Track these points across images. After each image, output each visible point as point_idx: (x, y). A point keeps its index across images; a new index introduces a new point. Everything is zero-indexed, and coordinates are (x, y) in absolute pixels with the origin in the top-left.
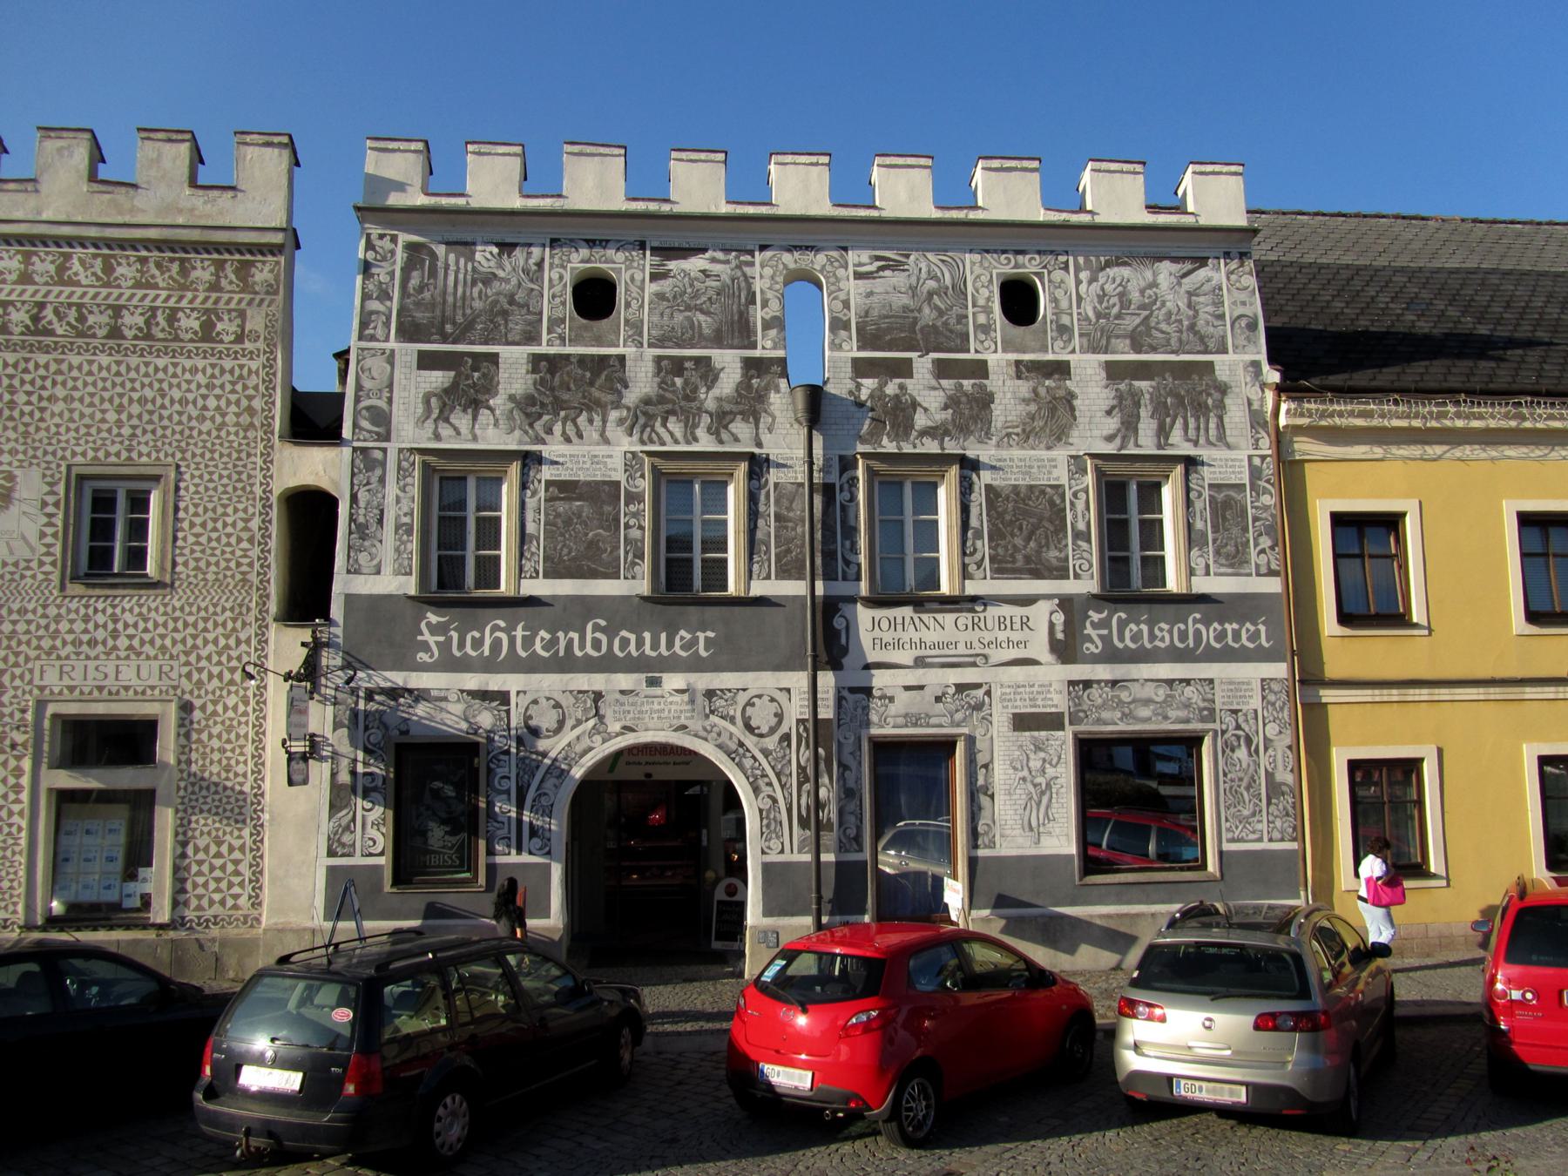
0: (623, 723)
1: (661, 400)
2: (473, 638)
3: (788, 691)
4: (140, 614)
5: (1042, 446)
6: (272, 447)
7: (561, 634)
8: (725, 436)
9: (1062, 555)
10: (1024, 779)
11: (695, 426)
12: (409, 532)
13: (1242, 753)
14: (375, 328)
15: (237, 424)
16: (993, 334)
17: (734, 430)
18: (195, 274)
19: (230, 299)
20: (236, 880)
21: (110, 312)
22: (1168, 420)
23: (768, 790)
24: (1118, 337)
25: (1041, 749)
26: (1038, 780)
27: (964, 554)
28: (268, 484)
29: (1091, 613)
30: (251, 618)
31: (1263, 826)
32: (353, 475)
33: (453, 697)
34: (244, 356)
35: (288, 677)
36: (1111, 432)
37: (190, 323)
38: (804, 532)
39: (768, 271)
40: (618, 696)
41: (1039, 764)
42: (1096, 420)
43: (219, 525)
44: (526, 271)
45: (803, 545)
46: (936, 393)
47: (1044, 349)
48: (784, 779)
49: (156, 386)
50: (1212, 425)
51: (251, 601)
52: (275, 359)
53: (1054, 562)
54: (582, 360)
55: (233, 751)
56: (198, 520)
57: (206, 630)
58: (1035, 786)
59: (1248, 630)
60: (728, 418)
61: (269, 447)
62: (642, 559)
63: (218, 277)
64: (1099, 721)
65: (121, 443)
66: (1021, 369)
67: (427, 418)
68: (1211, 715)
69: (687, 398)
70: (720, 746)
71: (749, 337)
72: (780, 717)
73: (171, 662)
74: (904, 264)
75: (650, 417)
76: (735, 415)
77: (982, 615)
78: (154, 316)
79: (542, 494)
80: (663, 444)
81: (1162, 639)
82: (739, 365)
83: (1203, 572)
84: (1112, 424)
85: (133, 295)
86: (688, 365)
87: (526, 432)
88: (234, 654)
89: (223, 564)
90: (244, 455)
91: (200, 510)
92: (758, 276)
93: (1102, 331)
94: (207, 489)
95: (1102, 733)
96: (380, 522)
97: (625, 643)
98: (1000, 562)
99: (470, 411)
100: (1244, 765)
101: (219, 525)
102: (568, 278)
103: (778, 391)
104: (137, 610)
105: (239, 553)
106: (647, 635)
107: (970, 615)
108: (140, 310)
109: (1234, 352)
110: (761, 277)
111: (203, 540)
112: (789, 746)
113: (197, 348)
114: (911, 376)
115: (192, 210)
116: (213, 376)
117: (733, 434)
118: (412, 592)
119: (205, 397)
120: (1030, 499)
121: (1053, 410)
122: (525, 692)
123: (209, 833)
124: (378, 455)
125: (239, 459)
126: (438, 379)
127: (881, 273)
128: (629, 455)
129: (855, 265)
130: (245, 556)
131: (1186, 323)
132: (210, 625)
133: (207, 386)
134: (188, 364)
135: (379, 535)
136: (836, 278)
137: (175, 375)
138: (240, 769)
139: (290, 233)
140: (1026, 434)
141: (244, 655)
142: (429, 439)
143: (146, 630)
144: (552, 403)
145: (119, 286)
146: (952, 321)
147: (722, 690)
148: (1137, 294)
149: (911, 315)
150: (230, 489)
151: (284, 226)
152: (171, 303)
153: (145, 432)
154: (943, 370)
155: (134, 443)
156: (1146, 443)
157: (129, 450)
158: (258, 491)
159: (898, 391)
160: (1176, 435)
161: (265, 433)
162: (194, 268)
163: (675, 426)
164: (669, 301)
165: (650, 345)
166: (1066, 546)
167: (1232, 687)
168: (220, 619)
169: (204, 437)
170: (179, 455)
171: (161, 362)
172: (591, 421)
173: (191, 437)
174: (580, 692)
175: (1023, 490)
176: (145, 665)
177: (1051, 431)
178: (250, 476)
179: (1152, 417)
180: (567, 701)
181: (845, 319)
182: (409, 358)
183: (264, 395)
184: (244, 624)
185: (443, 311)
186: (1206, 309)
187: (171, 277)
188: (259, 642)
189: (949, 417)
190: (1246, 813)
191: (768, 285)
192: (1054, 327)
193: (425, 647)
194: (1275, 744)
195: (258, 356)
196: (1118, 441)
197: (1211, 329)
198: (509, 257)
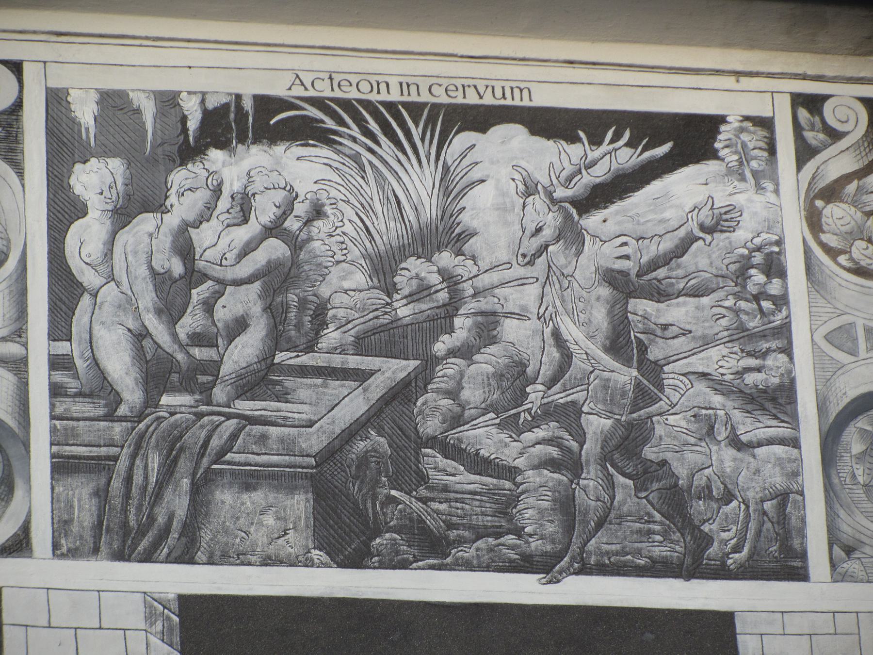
109: (838, 575)
148: (359, 279)
186: (697, 363)
197: (727, 457)
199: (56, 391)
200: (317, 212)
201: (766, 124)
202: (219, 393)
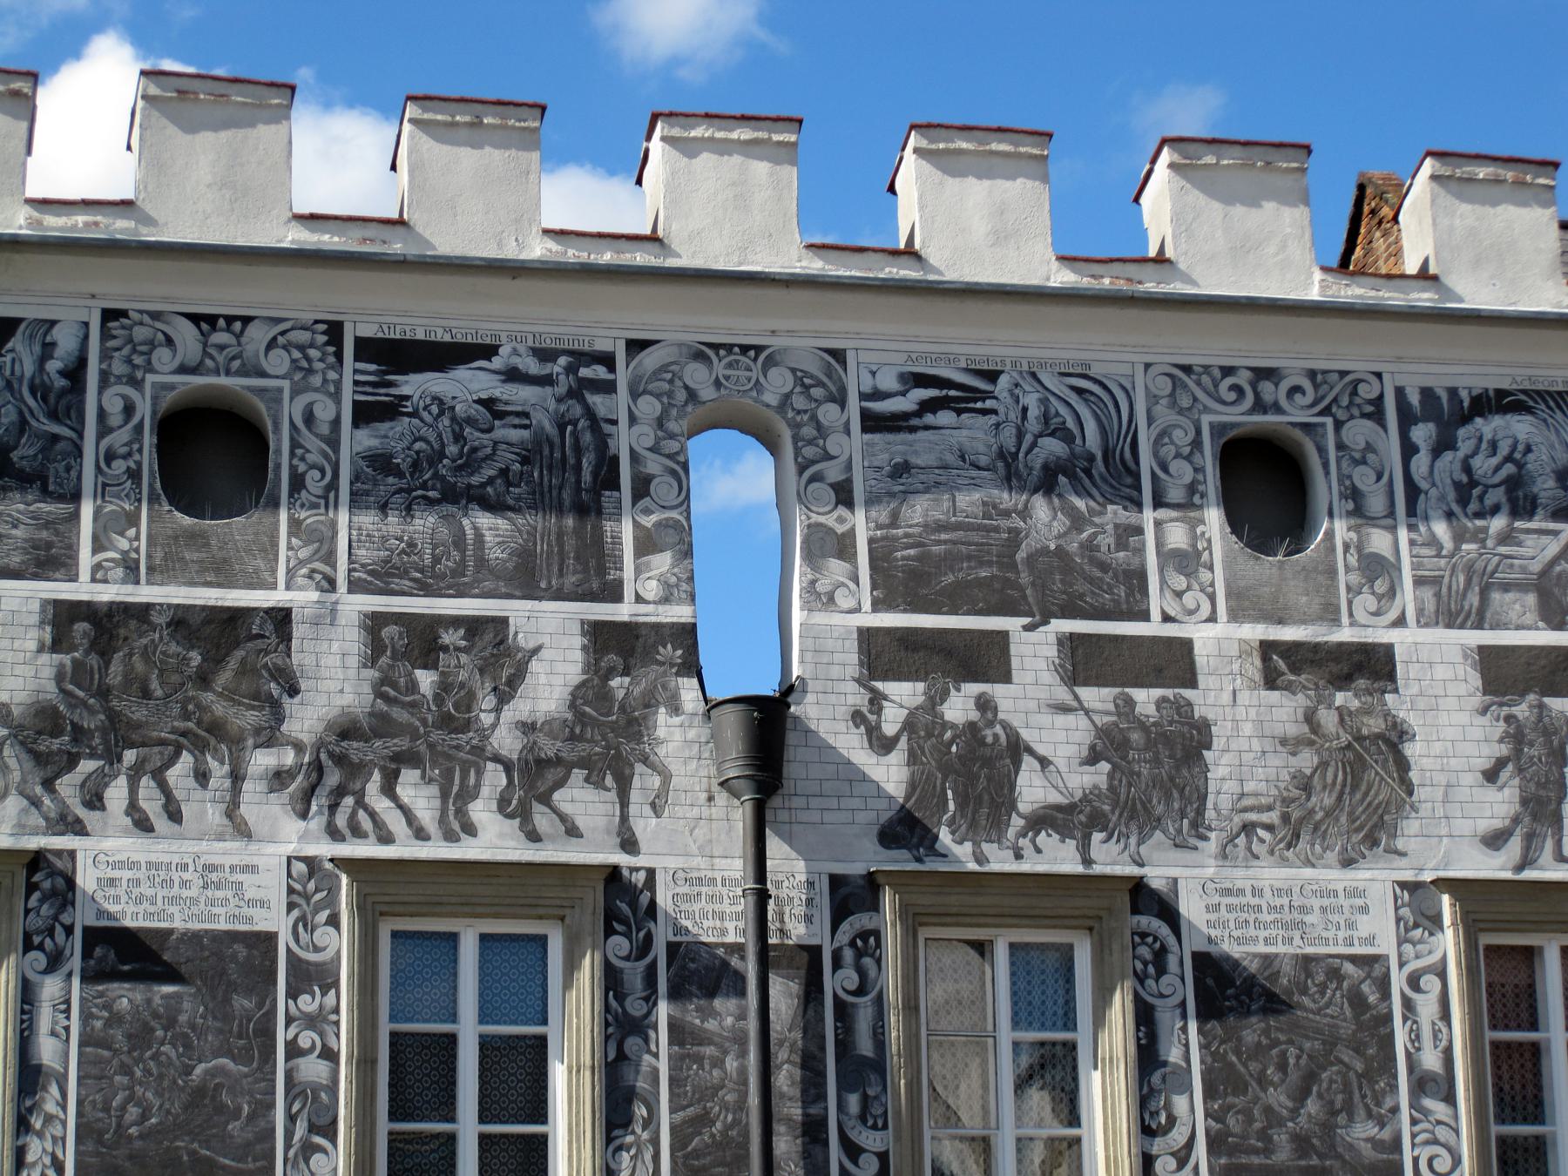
1: (381, 726)
8: (542, 819)
9: (1386, 1134)
11: (469, 794)
16: (1205, 575)
17: (566, 808)
24: (1506, 587)
27: (1147, 1131)
36: (1498, 824)
38: (743, 1071)
39: (649, 407)
42: (1462, 794)
44: (40, 389)
45: (741, 1105)
46: (1070, 720)
47: (1330, 615)
53: (1367, 1151)
54: (183, 621)
60: (551, 775)
62: (330, 1132)
69: (447, 722)
71: (602, 571)
74: (986, 395)
75: (354, 771)
76: (572, 765)
79: (76, 962)
80: (386, 838)
82: (578, 641)
84: (1500, 804)
86: (449, 637)
87: (35, 803)
93: (1470, 570)
98: (1233, 1151)
102: (144, 409)
103: (676, 709)
110: (633, 420)
114: (1006, 678)
117: (563, 818)
120: (1304, 991)
121: (1355, 769)
127: (929, 419)
128: (300, 868)
129: (863, 397)
136: (819, 426)
144: (104, 733)
146: (1106, 540)
148: (1551, 483)
149: (1004, 523)
159: (974, 715)
163: (417, 793)
164: (400, 475)
165: (355, 587)
166: (1395, 1110)
172: (202, 777)
175: (1287, 968)
177: (1352, 819)
181: (840, 529)
191: (650, 443)
192: (1353, 560)
196: (1515, 846)
199: (1412, 543)
200: (1528, 449)
202: (1490, 543)
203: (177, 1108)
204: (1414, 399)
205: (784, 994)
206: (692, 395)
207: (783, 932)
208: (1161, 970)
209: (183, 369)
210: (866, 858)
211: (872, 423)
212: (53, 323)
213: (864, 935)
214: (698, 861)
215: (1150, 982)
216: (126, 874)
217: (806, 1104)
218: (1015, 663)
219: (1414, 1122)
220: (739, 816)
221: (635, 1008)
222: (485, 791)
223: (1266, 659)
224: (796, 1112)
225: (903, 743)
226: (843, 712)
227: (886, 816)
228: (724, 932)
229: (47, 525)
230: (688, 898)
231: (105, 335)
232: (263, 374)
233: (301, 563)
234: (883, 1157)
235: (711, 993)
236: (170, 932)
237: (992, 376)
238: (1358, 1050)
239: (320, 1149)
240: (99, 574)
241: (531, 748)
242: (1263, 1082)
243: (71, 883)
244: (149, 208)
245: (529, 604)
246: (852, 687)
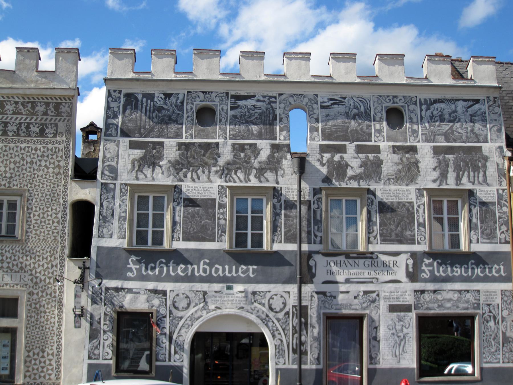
0: (216, 305)
1: (234, 163)
2: (151, 266)
3: (289, 292)
4: (12, 253)
5: (404, 184)
6: (68, 182)
7: (189, 266)
8: (262, 179)
9: (412, 234)
10: (393, 334)
11: (249, 174)
12: (125, 220)
13: (492, 324)
14: (111, 131)
15: (53, 172)
16: (383, 134)
17: (267, 177)
18: (37, 108)
19: (52, 119)
20: (50, 368)
21: (3, 125)
22: (461, 173)
23: (278, 336)
24: (439, 135)
25: (401, 321)
26: (400, 334)
27: (369, 233)
28: (66, 198)
29: (425, 260)
30: (58, 256)
31: (500, 356)
32: (101, 195)
33: (142, 292)
34: (56, 143)
35: (75, 282)
36: (435, 178)
37: (35, 129)
38: (296, 222)
39: (282, 105)
40: (214, 293)
41: (400, 327)
42: (429, 173)
43: (45, 216)
44: (176, 106)
45: (296, 228)
46: (357, 160)
48: (286, 332)
49: (21, 156)
50: (481, 175)
51: (58, 248)
52: (69, 145)
53: (409, 237)
54: (200, 145)
55: (49, 312)
56: (37, 214)
57: (39, 260)
58: (398, 337)
59: (495, 268)
60: (264, 171)
61: (66, 182)
62: (225, 232)
63: (47, 110)
64: (428, 308)
65: (6, 180)
66: (396, 150)
67: (133, 170)
68: (478, 306)
69: (246, 162)
70: (258, 317)
71: (273, 135)
72: (285, 304)
73: (25, 274)
74: (343, 102)
75: (230, 171)
76: (267, 169)
77: (376, 260)
78: (20, 126)
79: (182, 204)
80: (235, 182)
81: (457, 272)
82: (269, 147)
83: (476, 241)
84: (436, 174)
85: (12, 118)
86: (246, 147)
87: (175, 177)
88: (51, 271)
89: (47, 232)
90: (56, 186)
91: (38, 209)
92: (278, 108)
93: (432, 132)
94: (40, 200)
95: (429, 314)
96: (112, 215)
97: (217, 270)
98: (384, 236)
99: (151, 167)
100: (493, 329)
101: (45, 216)
102: (194, 109)
103: (286, 159)
104: (11, 251)
105: (53, 228)
106: (227, 267)
107: (370, 260)
108: (15, 124)
109: (491, 142)
110: (279, 108)
111: (39, 222)
112: (289, 317)
113: (38, 140)
114: (346, 153)
115: (37, 81)
116: (44, 152)
117: (266, 178)
118: (126, 246)
119: (40, 161)
120: (398, 208)
121: (409, 168)
122: (173, 291)
123: (39, 347)
124: (112, 186)
125: (54, 187)
126: (138, 153)
127: (333, 106)
129: (321, 103)
130: (56, 229)
131: (469, 129)
132: (41, 258)
133: (41, 156)
134: (34, 146)
135: (112, 221)
136: (313, 108)
137: (28, 151)
138: (52, 320)
139: (76, 90)
140: (398, 178)
141: (55, 272)
142: (134, 180)
143: (15, 260)
145: (7, 114)
146: (365, 128)
147: (259, 292)
150: (50, 200)
151: (74, 88)
152: (28, 121)
153: (16, 175)
154: (360, 150)
155: (11, 180)
156: (451, 183)
157: (9, 183)
158: (61, 201)
159: (340, 159)
160: (465, 180)
161: (65, 176)
162: (37, 106)
163: (241, 174)
165: (230, 138)
166: (414, 229)
167: (488, 294)
168: (45, 256)
169: (40, 178)
170: (29, 186)
171: (23, 146)
172: (204, 172)
173: (34, 178)
174: (197, 291)
176: (14, 274)
177: (408, 177)
178: (58, 195)
179: (454, 171)
180: (191, 295)
181: (316, 126)
182: (125, 144)
183: (65, 160)
184: (55, 258)
185: (141, 124)
187: (28, 110)
188: (61, 266)
189: (363, 171)
190: (493, 350)
191: (282, 112)
192: (410, 130)
193: (131, 270)
194: (507, 319)
195: (63, 143)
197: (481, 132)
198: (169, 99)
201: (484, 100)
203: (199, 228)
204: (423, 101)
205: (304, 209)
206: (290, 103)
207: (304, 198)
208: (372, 204)
209: (201, 101)
210: (320, 185)
211: (323, 107)
212: (178, 94)
213: (319, 198)
214: (290, 186)
215: (370, 207)
216: (191, 189)
217: (308, 228)
218: (347, 150)
219: (418, 231)
220: (296, 177)
221: (278, 211)
222: (252, 174)
223: (393, 148)
224: (306, 229)
225: (327, 164)
226: (316, 159)
227: (323, 178)
228: (294, 198)
229: (177, 129)
230: (288, 192)
231: (188, 96)
232: (215, 102)
233: (221, 135)
234: (321, 237)
235: (291, 209)
236: (198, 199)
237: (345, 98)
238: (408, 218)
239: (223, 235)
240: (186, 137)
241: (261, 166)
242: (390, 224)
243: (181, 190)
244: (195, 73)
245: (260, 141)
246: (318, 154)
